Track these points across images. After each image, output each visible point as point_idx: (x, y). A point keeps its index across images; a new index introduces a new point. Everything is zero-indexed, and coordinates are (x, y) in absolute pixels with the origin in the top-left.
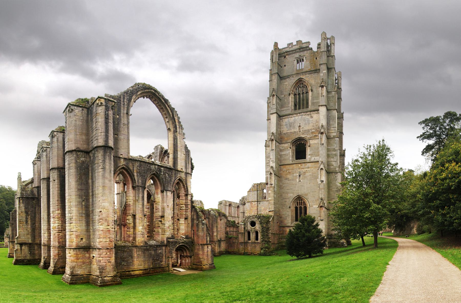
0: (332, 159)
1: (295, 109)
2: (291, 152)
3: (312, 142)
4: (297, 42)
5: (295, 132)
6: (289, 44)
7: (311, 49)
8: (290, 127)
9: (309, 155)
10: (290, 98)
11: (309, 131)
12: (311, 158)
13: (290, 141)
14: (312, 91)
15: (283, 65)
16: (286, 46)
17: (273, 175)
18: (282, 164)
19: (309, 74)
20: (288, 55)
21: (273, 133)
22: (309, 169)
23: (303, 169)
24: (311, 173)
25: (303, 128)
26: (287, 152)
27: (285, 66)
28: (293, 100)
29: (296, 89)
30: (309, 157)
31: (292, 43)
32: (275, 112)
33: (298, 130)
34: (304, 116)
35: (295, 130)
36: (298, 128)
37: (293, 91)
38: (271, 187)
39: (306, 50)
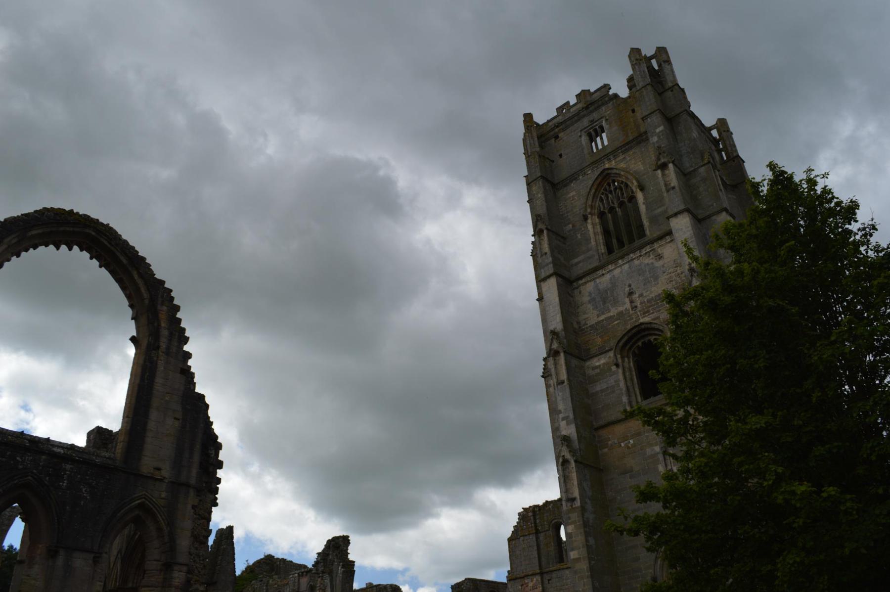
1: (610, 250)
2: (621, 377)
5: (621, 314)
7: (616, 96)
8: (604, 302)
10: (590, 227)
13: (613, 343)
14: (642, 189)
16: (555, 114)
17: (572, 462)
18: (601, 423)
19: (623, 153)
20: (563, 130)
25: (641, 295)
26: (612, 381)
27: (561, 156)
28: (599, 229)
29: (602, 200)
31: (568, 103)
32: (551, 271)
33: (628, 305)
34: (636, 262)
35: (621, 309)
36: (627, 300)
38: (573, 510)
39: (603, 104)
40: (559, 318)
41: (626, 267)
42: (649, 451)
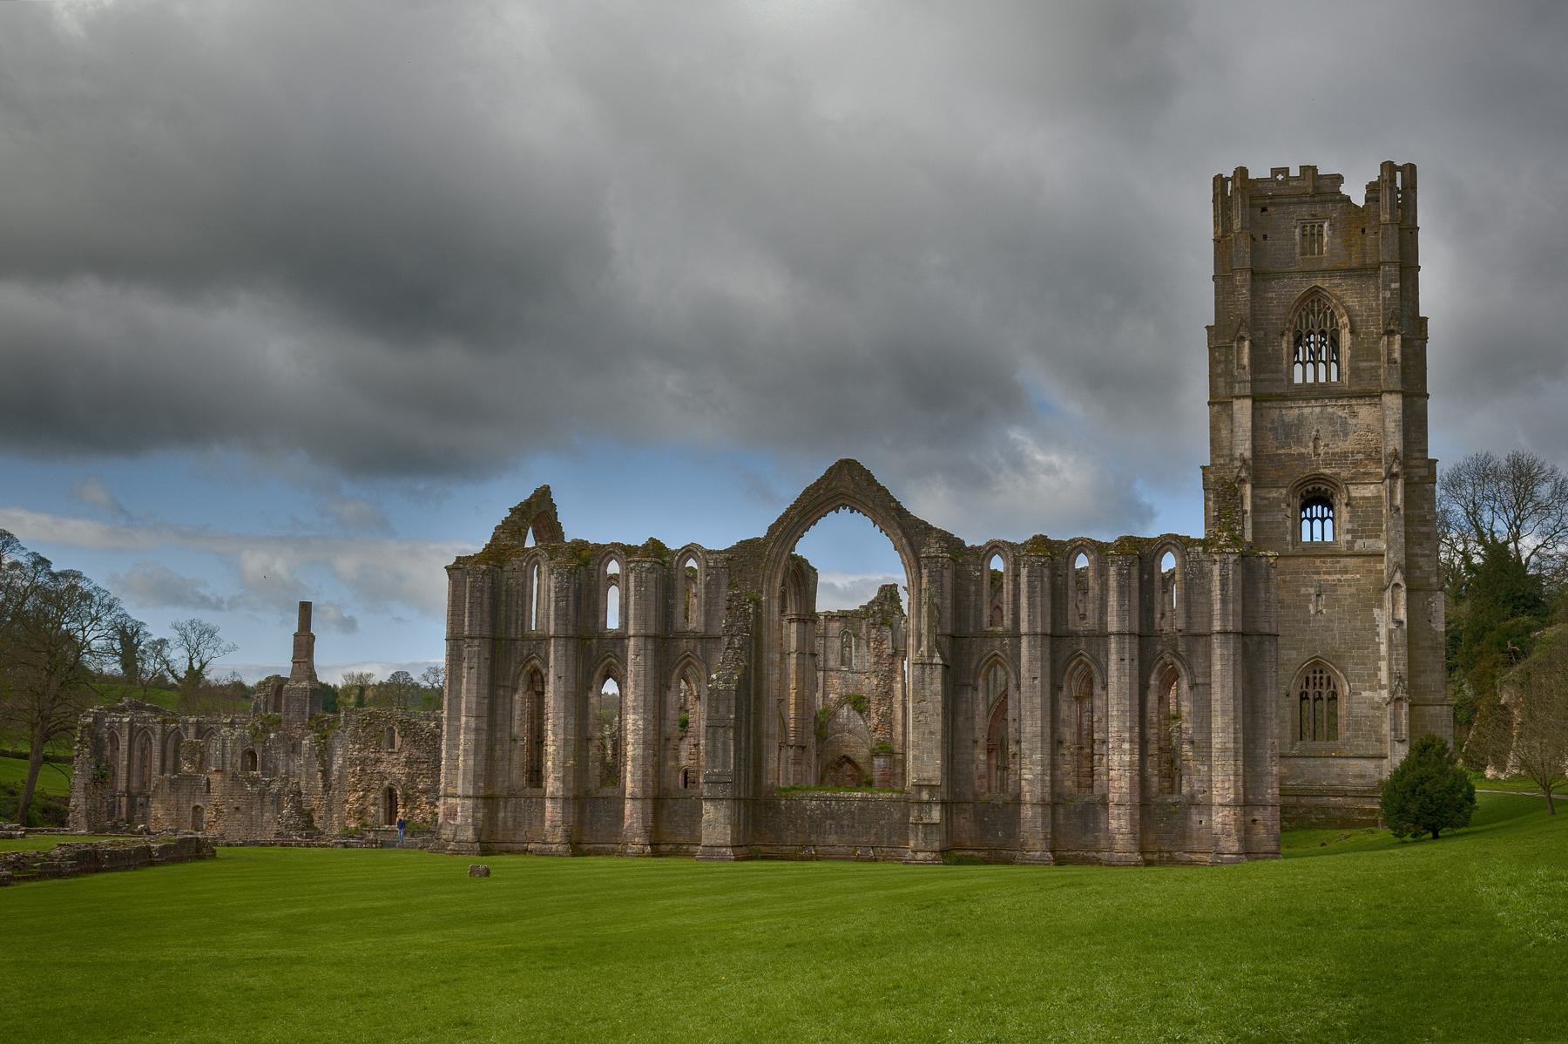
0: (1417, 550)
3: (1358, 492)
4: (1303, 169)
5: (1301, 455)
6: (1275, 171)
9: (1348, 532)
11: (1345, 455)
12: (1351, 544)
14: (1352, 332)
15: (1259, 237)
21: (1244, 461)
22: (1349, 576)
23: (1329, 573)
24: (1353, 590)
26: (1280, 517)
27: (1265, 237)
30: (1349, 537)
33: (1311, 449)
34: (1330, 410)
37: (1291, 322)
40: (1248, 444)
41: (1318, 410)
42: (1303, 590)
